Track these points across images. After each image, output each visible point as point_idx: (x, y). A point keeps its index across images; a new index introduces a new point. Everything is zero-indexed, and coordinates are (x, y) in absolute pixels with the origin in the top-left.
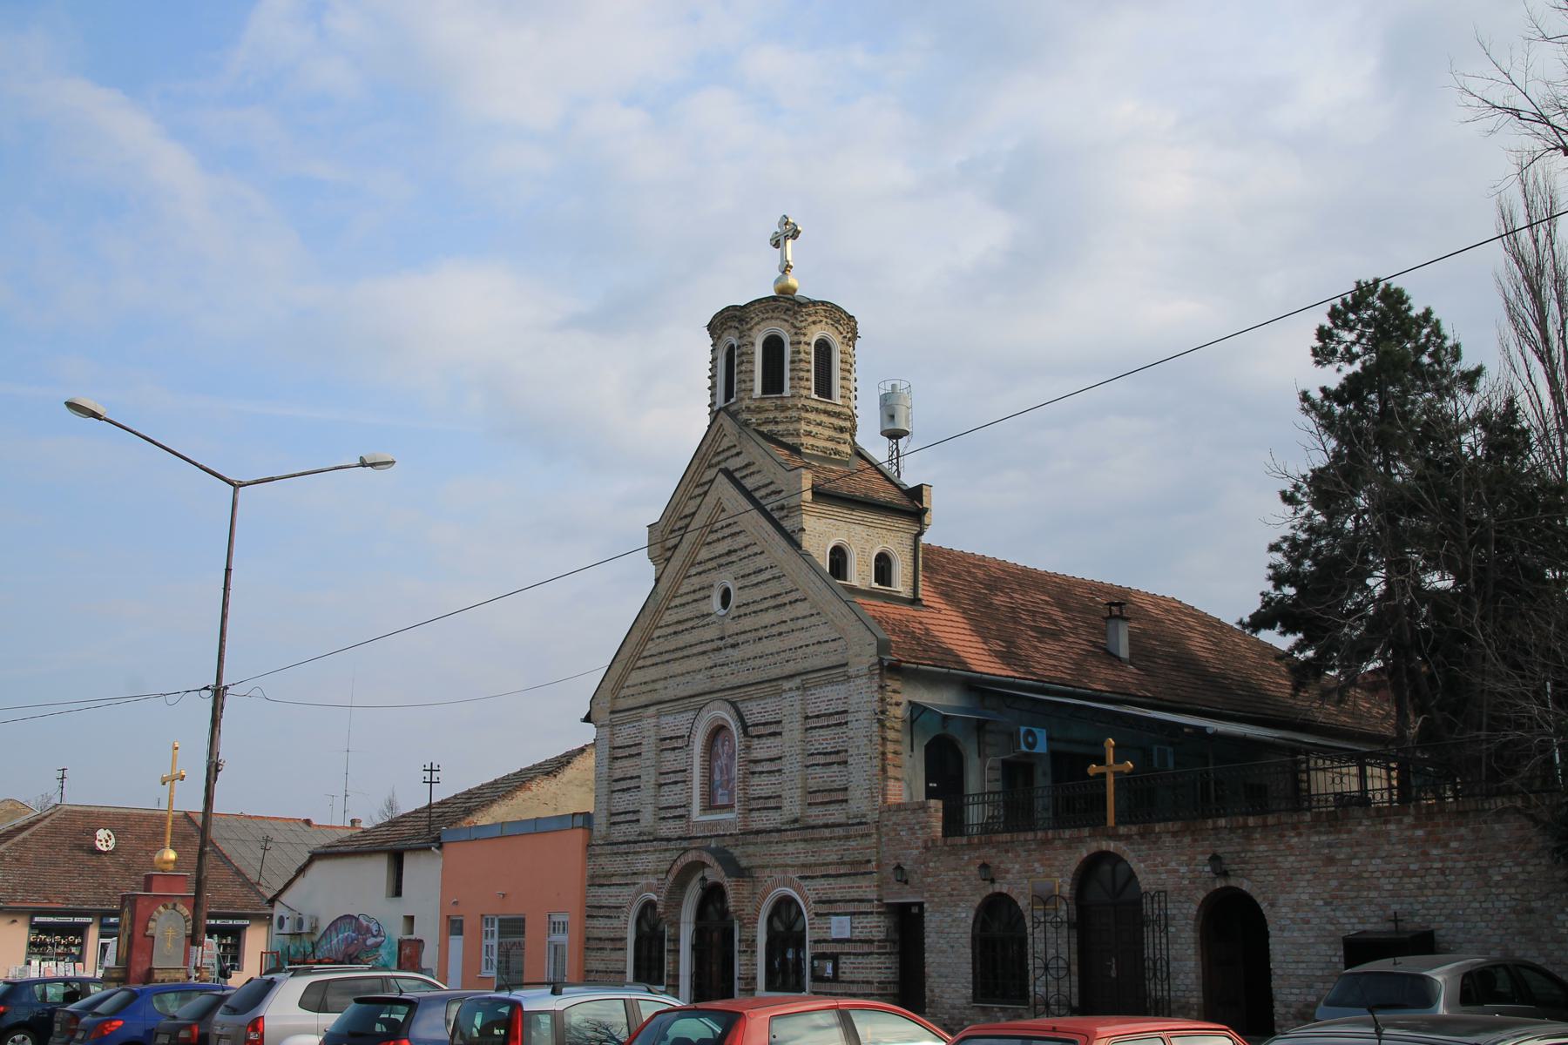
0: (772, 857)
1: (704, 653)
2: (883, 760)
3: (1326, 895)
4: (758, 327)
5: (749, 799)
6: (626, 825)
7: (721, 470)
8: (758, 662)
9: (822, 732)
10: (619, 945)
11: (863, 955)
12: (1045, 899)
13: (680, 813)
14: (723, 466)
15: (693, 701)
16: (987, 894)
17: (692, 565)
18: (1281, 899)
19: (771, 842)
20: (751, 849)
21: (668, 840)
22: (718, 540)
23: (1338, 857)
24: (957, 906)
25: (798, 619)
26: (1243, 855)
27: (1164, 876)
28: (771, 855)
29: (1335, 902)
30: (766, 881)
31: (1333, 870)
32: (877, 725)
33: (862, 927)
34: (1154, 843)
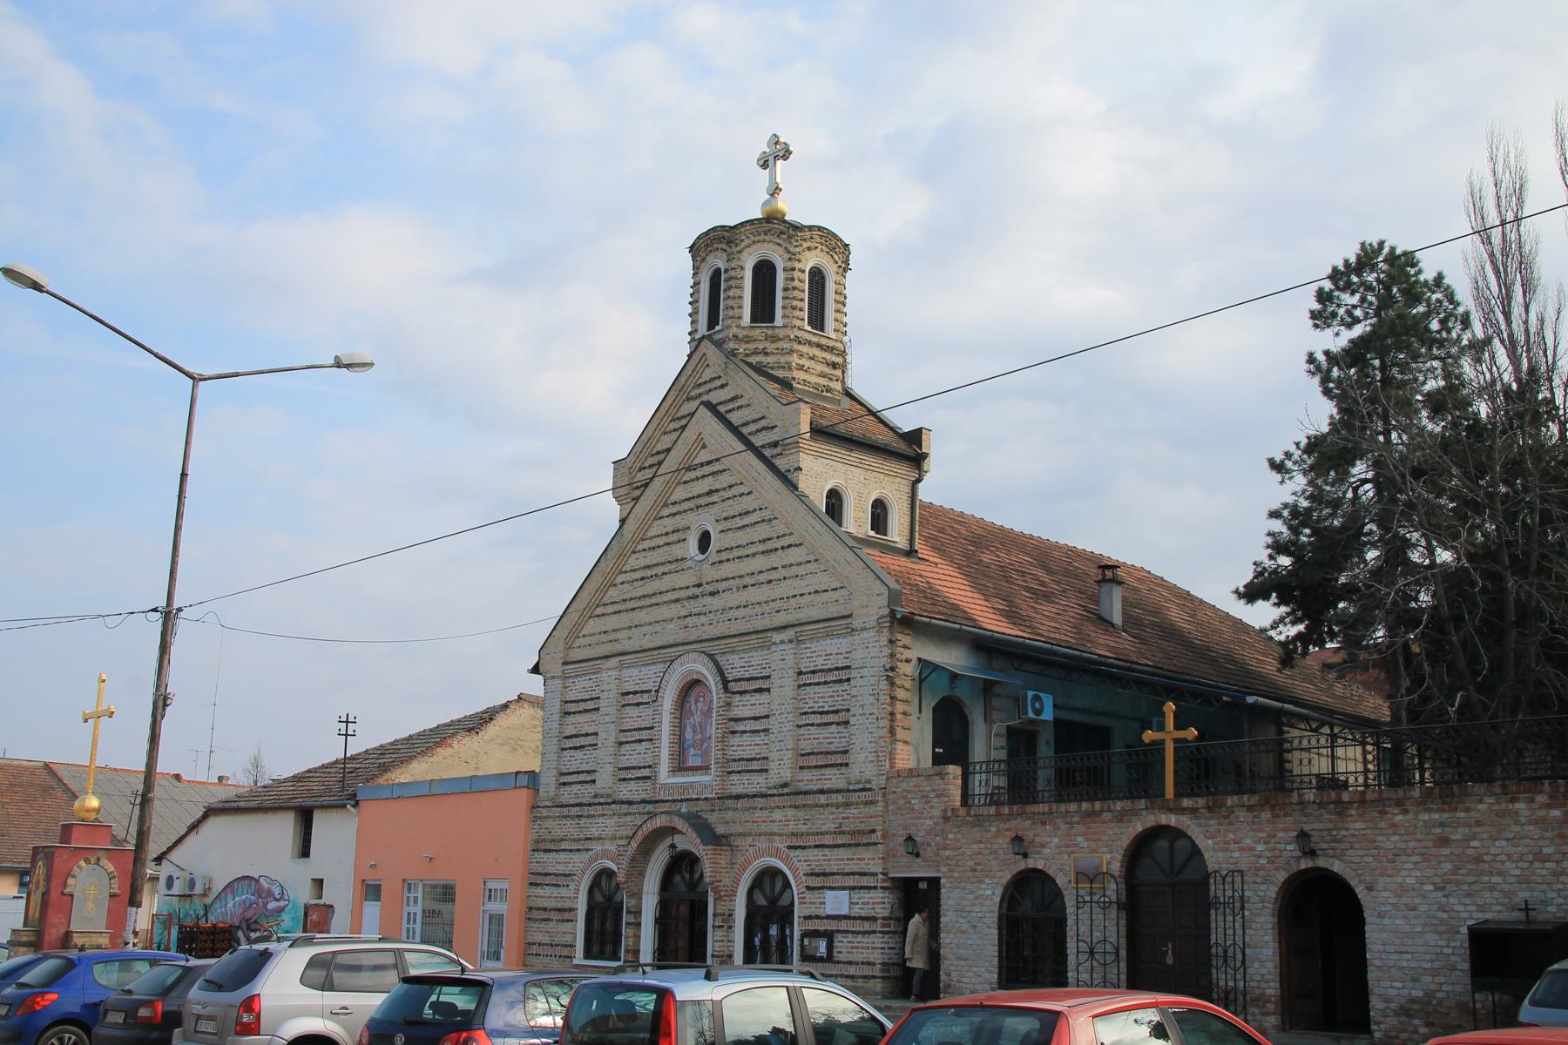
1: (677, 600)
2: (892, 721)
3: (1437, 880)
4: (749, 250)
5: (728, 761)
6: (579, 786)
7: (702, 403)
8: (742, 612)
9: (817, 689)
10: (567, 916)
11: (864, 933)
12: (1089, 877)
13: (644, 775)
14: (705, 398)
15: (666, 653)
16: (1019, 869)
17: (665, 505)
18: (1382, 882)
19: (755, 808)
20: (730, 815)
21: (630, 803)
22: (697, 478)
23: (1452, 837)
24: (980, 882)
25: (791, 565)
26: (1335, 833)
27: (1236, 854)
28: (754, 822)
29: (1448, 887)
31: (1446, 851)
32: (886, 682)
33: (863, 903)
34: (1225, 817)
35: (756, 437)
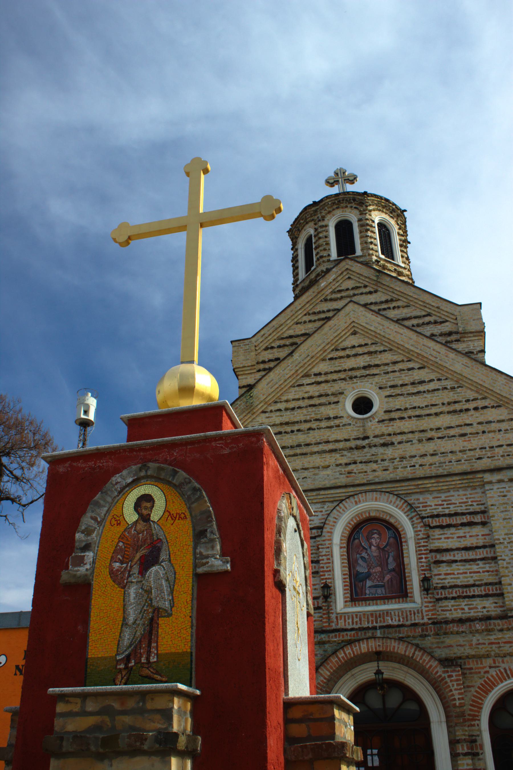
0: (494, 646)
8: (429, 459)
17: (307, 375)
22: (348, 356)
25: (490, 422)
30: (487, 672)
35: (421, 328)
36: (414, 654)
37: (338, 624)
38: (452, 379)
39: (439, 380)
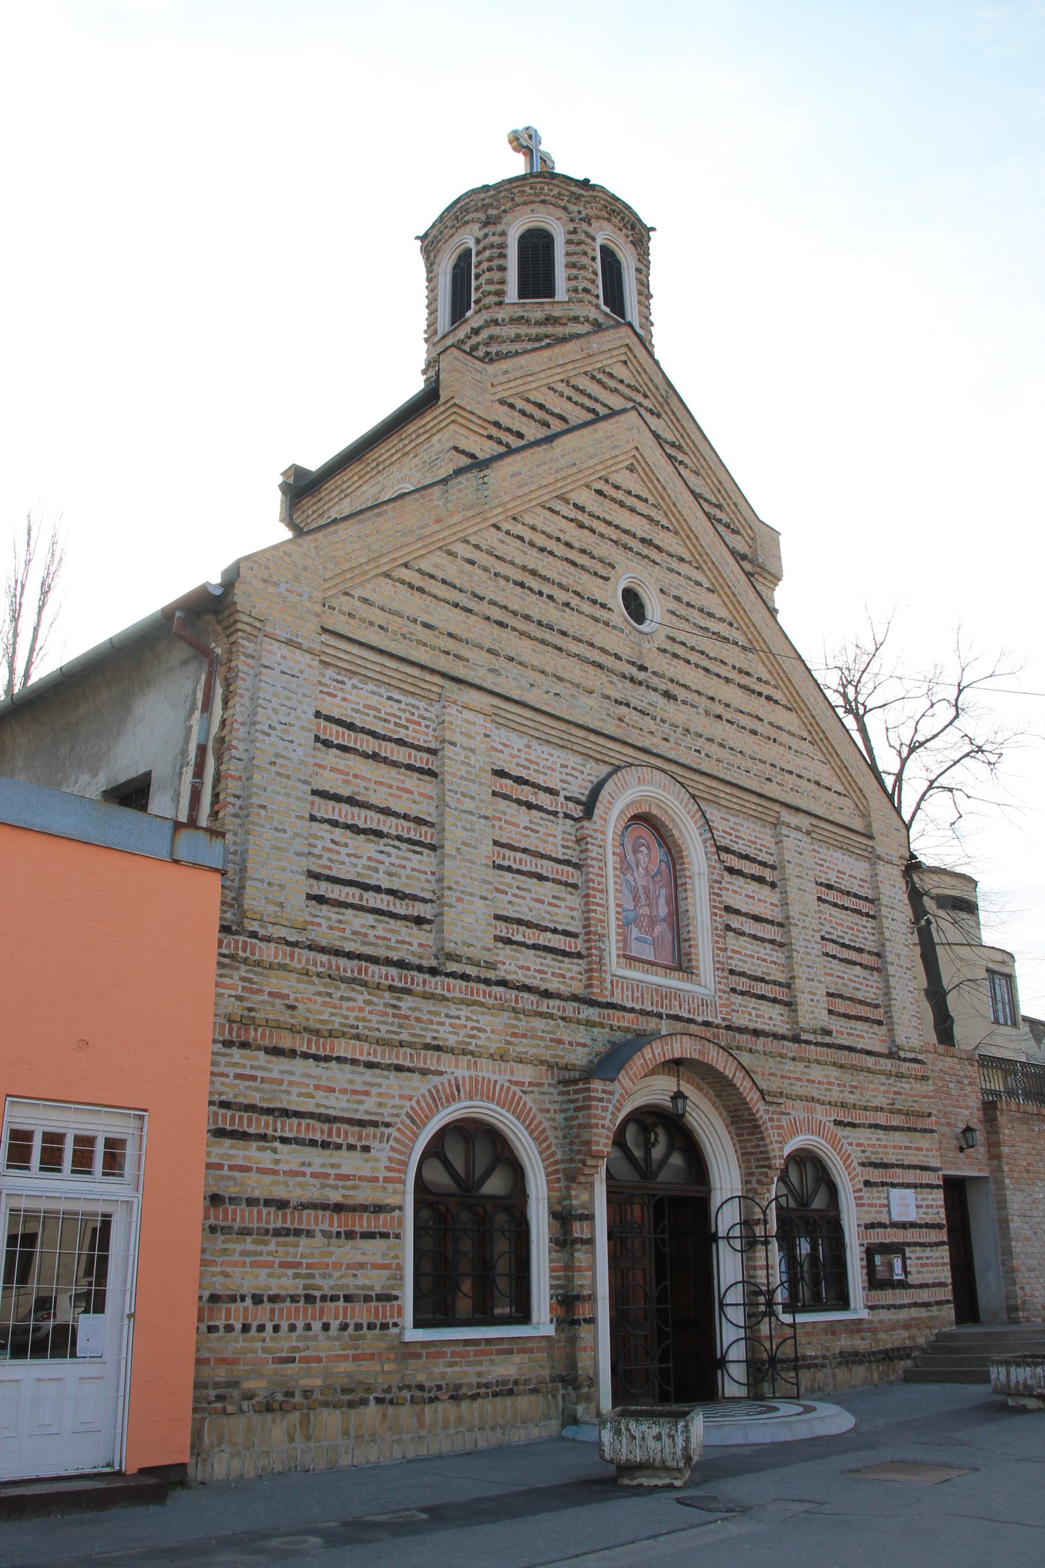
0: (786, 1081)
6: (370, 919)
8: (714, 749)
19: (782, 1056)
24: (1033, 1184)
28: (783, 1077)
36: (734, 1074)
37: (612, 995)
38: (745, 633)
39: (731, 624)
